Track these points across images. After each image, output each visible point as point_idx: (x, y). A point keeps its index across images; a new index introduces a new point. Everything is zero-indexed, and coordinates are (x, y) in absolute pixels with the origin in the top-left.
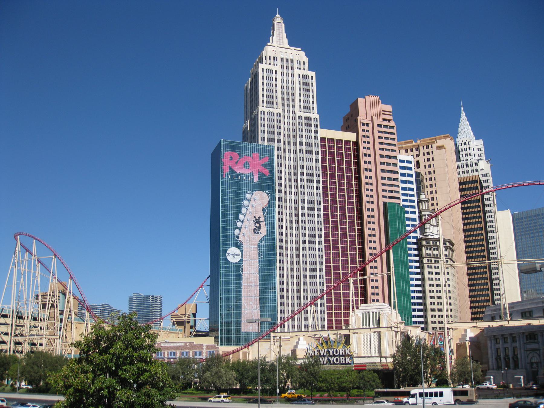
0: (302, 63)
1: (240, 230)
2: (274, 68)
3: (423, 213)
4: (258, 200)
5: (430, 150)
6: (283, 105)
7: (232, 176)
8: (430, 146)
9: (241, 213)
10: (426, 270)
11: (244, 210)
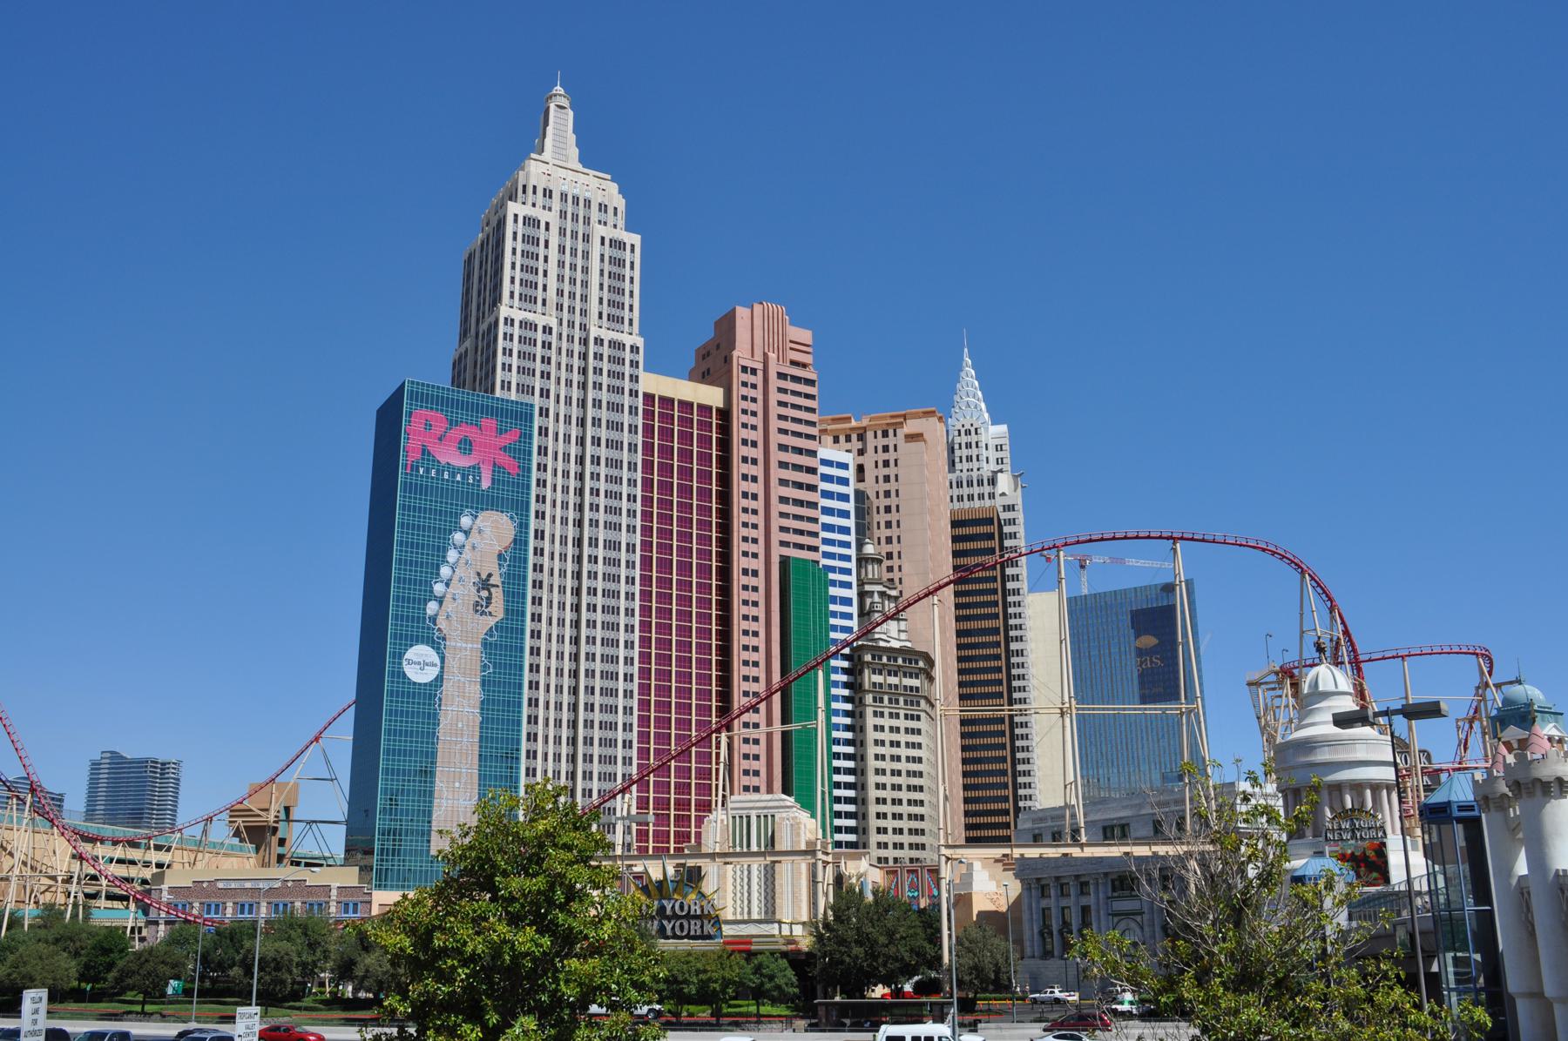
0: (611, 211)
1: (441, 603)
2: (544, 217)
3: (867, 588)
4: (487, 531)
5: (890, 441)
6: (560, 307)
7: (428, 471)
8: (891, 432)
9: (445, 561)
10: (871, 721)
11: (452, 555)
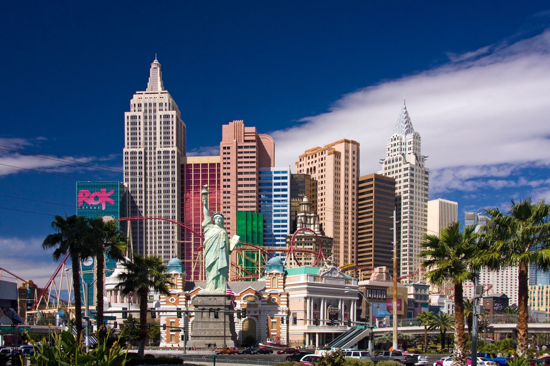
2: (137, 114)
